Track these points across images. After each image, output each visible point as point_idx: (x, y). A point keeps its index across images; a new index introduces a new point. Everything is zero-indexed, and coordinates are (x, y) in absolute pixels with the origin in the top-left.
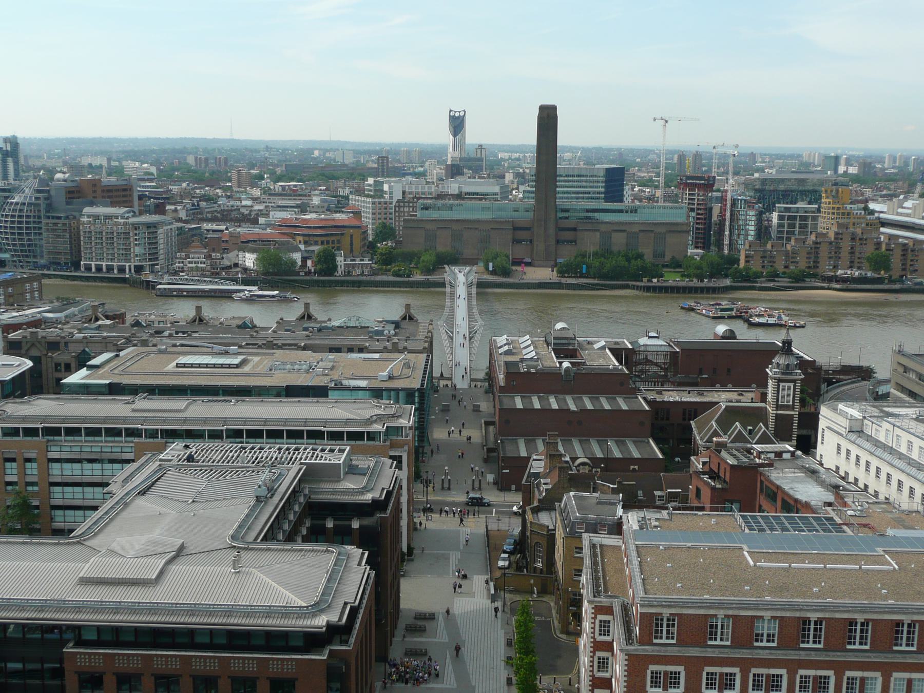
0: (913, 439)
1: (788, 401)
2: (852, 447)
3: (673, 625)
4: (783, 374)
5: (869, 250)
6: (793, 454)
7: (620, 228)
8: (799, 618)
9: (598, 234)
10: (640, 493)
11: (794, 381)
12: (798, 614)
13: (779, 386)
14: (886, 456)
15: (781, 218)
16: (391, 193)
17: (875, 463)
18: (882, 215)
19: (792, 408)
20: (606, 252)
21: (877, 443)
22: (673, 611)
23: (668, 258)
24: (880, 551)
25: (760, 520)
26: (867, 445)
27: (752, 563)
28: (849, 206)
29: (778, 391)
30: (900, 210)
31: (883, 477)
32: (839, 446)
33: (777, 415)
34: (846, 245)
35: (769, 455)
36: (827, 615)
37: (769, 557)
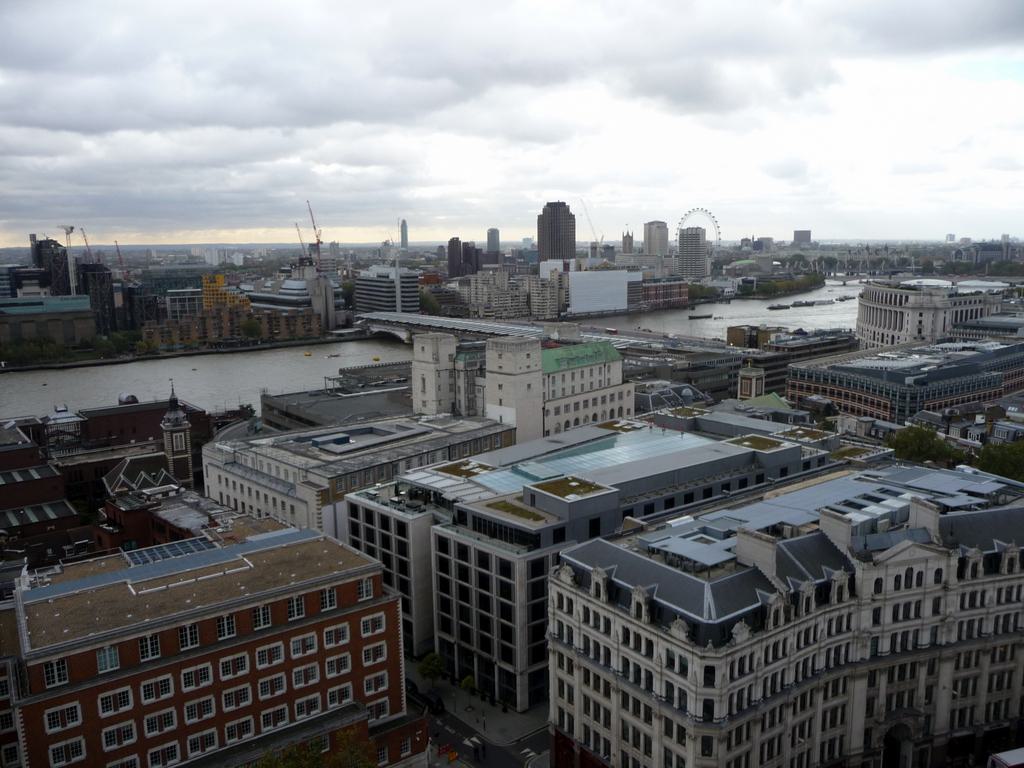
2: (229, 476)
3: (64, 668)
4: (174, 426)
5: (244, 320)
6: (177, 491)
8: (176, 629)
10: (50, 551)
11: (184, 431)
12: (174, 626)
13: (172, 436)
14: (254, 478)
15: (173, 301)
17: (246, 485)
18: (251, 294)
19: (186, 452)
21: (247, 469)
22: (61, 656)
23: (78, 341)
24: (240, 556)
25: (145, 554)
26: (239, 472)
27: (134, 593)
30: (263, 289)
31: (254, 493)
32: (220, 477)
34: (225, 316)
35: (157, 496)
36: (199, 620)
37: (149, 584)
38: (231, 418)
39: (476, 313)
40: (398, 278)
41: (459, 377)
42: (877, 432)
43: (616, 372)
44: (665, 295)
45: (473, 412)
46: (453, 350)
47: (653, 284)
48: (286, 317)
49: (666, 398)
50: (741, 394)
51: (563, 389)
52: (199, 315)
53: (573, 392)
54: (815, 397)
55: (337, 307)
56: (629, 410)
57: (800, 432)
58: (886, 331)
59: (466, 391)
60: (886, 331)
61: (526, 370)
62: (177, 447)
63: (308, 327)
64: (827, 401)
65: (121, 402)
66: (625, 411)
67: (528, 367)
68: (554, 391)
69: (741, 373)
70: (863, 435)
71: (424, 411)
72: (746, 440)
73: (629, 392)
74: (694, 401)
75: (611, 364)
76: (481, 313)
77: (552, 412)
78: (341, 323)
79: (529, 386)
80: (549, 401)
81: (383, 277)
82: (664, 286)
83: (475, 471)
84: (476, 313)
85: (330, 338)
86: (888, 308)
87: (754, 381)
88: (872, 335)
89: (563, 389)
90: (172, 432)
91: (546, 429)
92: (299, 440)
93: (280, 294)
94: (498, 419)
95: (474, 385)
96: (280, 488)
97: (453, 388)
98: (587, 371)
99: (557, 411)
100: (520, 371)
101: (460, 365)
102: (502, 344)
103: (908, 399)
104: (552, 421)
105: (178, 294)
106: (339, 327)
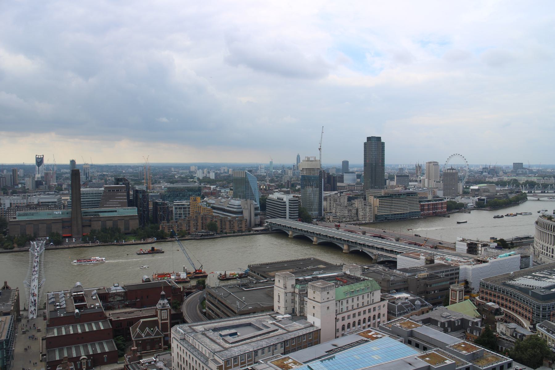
0: (199, 344)
1: (165, 317)
4: (162, 307)
5: (209, 221)
7: (110, 219)
9: (100, 222)
11: (167, 309)
13: (161, 312)
15: (176, 208)
16: (4, 204)
18: (214, 205)
19: (167, 319)
20: (104, 229)
26: (186, 345)
28: (200, 204)
29: (161, 314)
30: (220, 203)
33: (161, 323)
34: (200, 221)
38: (194, 289)
39: (329, 219)
40: (288, 200)
41: (296, 295)
42: (516, 334)
43: (378, 295)
44: (433, 209)
45: (303, 317)
46: (294, 282)
47: (426, 203)
48: (230, 221)
49: (406, 306)
50: (451, 299)
51: (347, 307)
52: (187, 219)
53: (352, 308)
54: (490, 304)
55: (256, 215)
56: (384, 315)
57: (463, 346)
58: (549, 246)
59: (300, 304)
60: (549, 246)
61: (326, 300)
62: (163, 317)
63: (240, 226)
64: (496, 306)
65: (143, 281)
66: (381, 315)
67: (328, 298)
68: (342, 309)
69: (452, 287)
70: (509, 335)
71: (279, 311)
72: (427, 356)
73: (384, 305)
74: (422, 306)
75: (375, 292)
76: (331, 220)
77: (341, 319)
78: (257, 223)
79: (328, 308)
80: (339, 314)
81: (280, 199)
82: (432, 204)
83: (290, 365)
84: (329, 219)
85: (252, 232)
86: (547, 232)
87: (458, 292)
88: (542, 246)
89: (347, 307)
90: (161, 310)
91: (337, 328)
92: (215, 330)
93: (228, 207)
94: (313, 324)
95: (304, 300)
96: (202, 359)
97: (293, 301)
98: (360, 297)
99: (343, 319)
100: (324, 301)
101: (297, 291)
102: (315, 287)
103: (541, 309)
104: (340, 324)
105: (178, 205)
106: (256, 225)
